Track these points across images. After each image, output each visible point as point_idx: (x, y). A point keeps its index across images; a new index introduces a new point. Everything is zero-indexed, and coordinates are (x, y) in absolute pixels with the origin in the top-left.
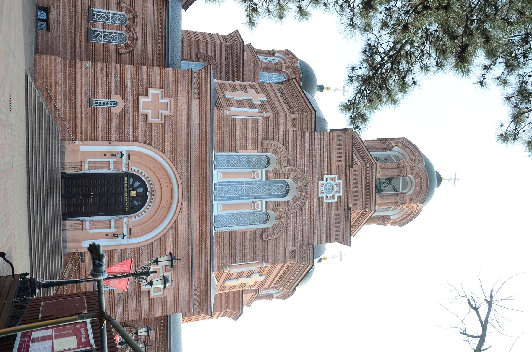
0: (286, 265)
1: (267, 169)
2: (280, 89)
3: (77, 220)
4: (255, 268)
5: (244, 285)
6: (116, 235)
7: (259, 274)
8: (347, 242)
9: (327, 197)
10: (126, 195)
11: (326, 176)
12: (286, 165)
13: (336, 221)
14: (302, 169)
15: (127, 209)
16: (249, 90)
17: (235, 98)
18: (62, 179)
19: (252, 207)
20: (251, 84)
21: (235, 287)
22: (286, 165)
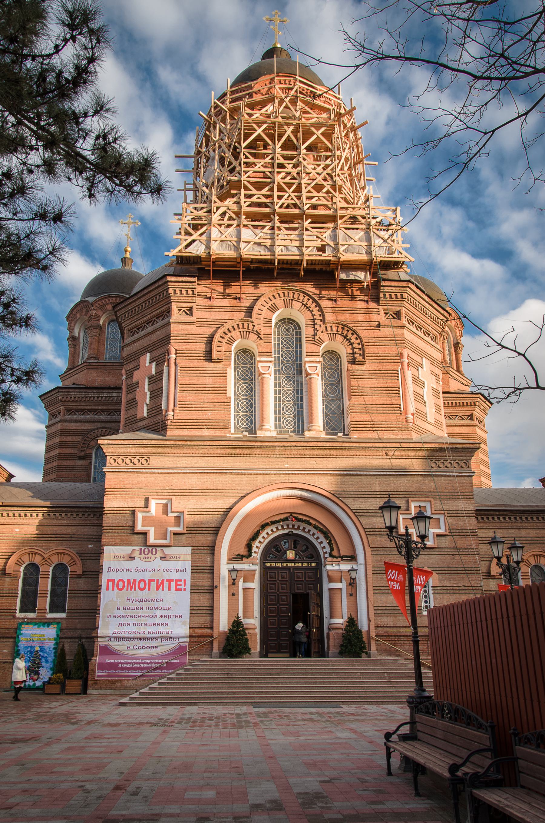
0: (408, 325)
1: (256, 354)
2: (131, 332)
3: (328, 634)
4: (409, 374)
5: (435, 392)
6: (352, 581)
7: (420, 368)
10: (293, 565)
12: (251, 324)
15: (313, 565)
16: (135, 380)
17: (148, 401)
18: (268, 657)
20: (124, 377)
21: (437, 406)
22: (251, 324)
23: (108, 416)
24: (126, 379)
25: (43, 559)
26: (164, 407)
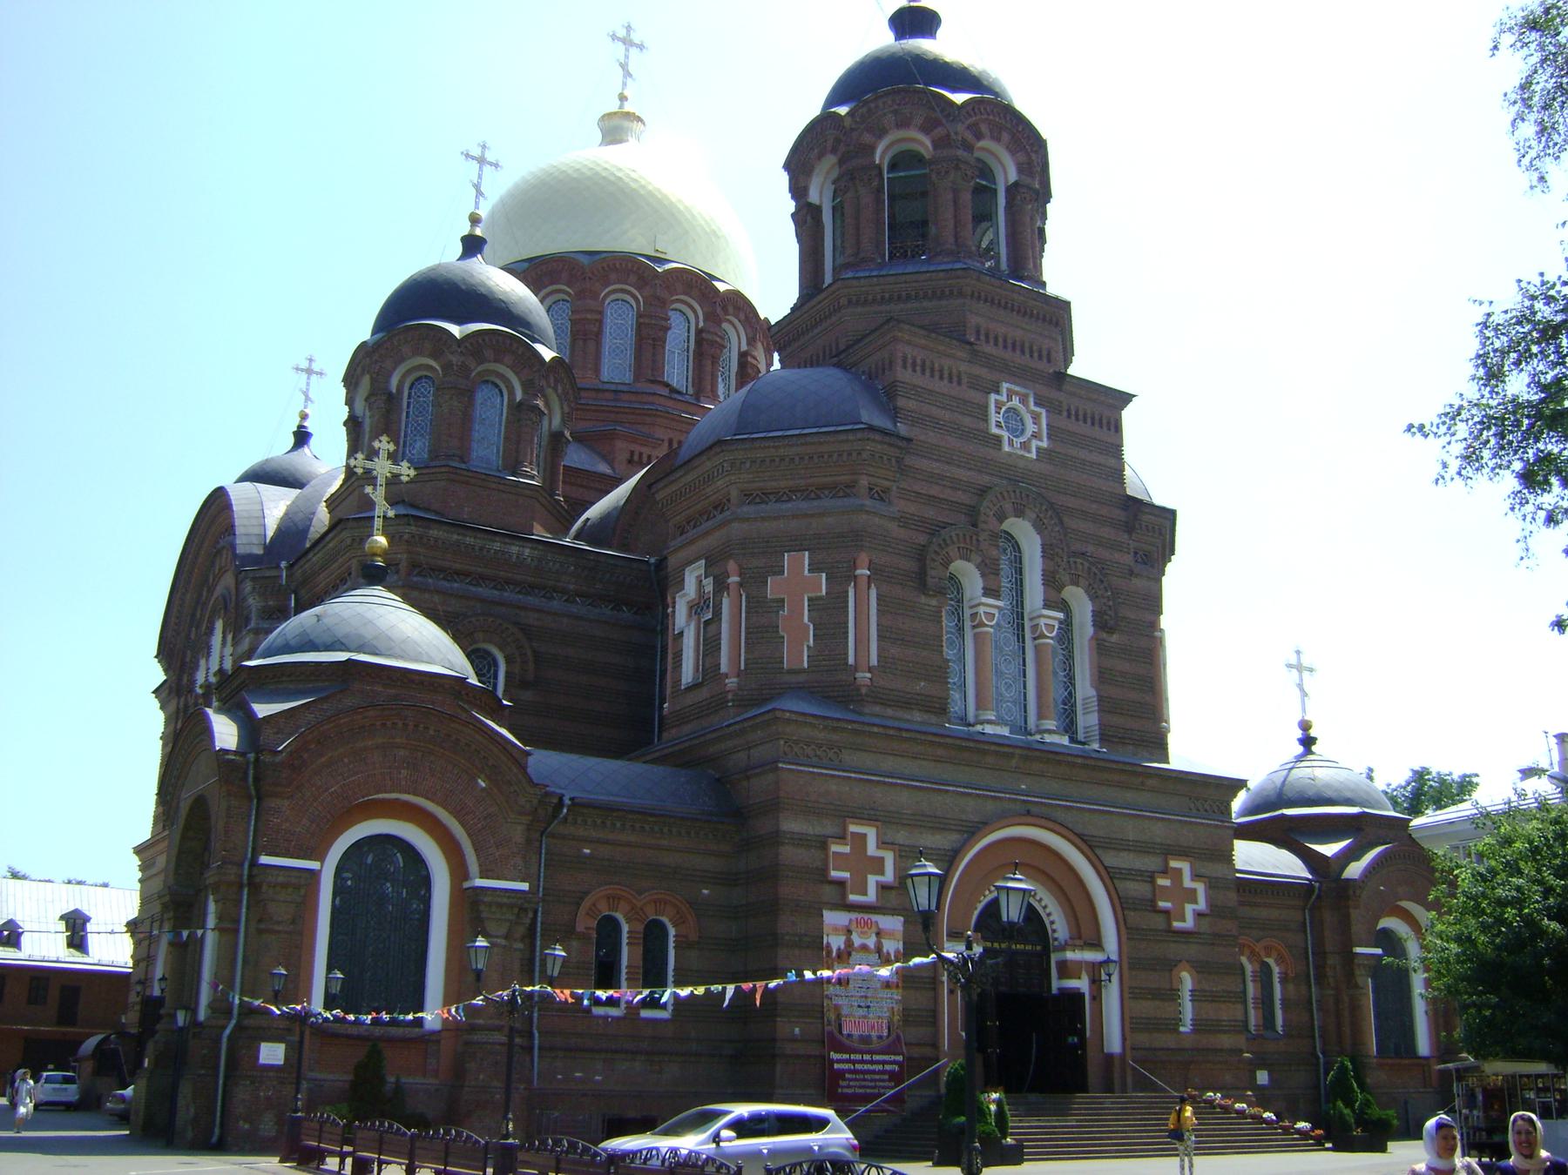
8: (1125, 398)
9: (1035, 436)
11: (994, 430)
13: (1081, 423)
14: (983, 491)
15: (1039, 948)
19: (1049, 644)
23: (496, 592)
24: (741, 585)
25: (633, 909)
26: (851, 660)
